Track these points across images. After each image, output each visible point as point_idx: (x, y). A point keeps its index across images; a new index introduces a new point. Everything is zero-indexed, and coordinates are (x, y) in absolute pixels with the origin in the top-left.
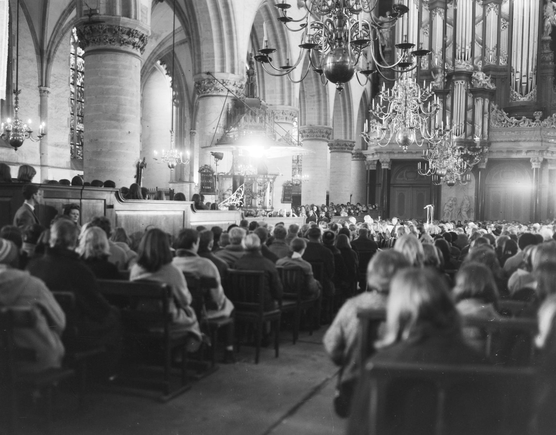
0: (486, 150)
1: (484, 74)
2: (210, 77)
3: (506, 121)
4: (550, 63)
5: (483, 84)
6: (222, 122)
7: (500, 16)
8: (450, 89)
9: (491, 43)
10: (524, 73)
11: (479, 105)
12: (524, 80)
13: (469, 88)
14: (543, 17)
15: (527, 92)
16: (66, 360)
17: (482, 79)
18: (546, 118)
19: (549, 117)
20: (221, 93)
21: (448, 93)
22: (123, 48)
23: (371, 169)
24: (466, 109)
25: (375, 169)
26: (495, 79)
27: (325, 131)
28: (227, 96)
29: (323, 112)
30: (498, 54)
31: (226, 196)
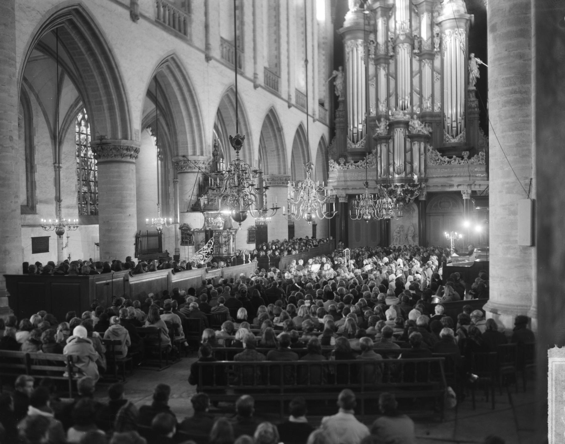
0: (423, 185)
1: (419, 122)
2: (185, 159)
4: (476, 109)
6: (195, 192)
7: (433, 69)
9: (427, 93)
10: (454, 119)
11: (416, 147)
12: (454, 124)
13: (407, 134)
14: (468, 71)
15: (457, 135)
16: (128, 356)
17: (417, 126)
19: (476, 156)
20: (194, 170)
21: (390, 138)
22: (123, 159)
24: (405, 152)
26: (431, 123)
27: (284, 179)
28: (198, 172)
29: (282, 163)
30: (433, 102)
31: (200, 246)
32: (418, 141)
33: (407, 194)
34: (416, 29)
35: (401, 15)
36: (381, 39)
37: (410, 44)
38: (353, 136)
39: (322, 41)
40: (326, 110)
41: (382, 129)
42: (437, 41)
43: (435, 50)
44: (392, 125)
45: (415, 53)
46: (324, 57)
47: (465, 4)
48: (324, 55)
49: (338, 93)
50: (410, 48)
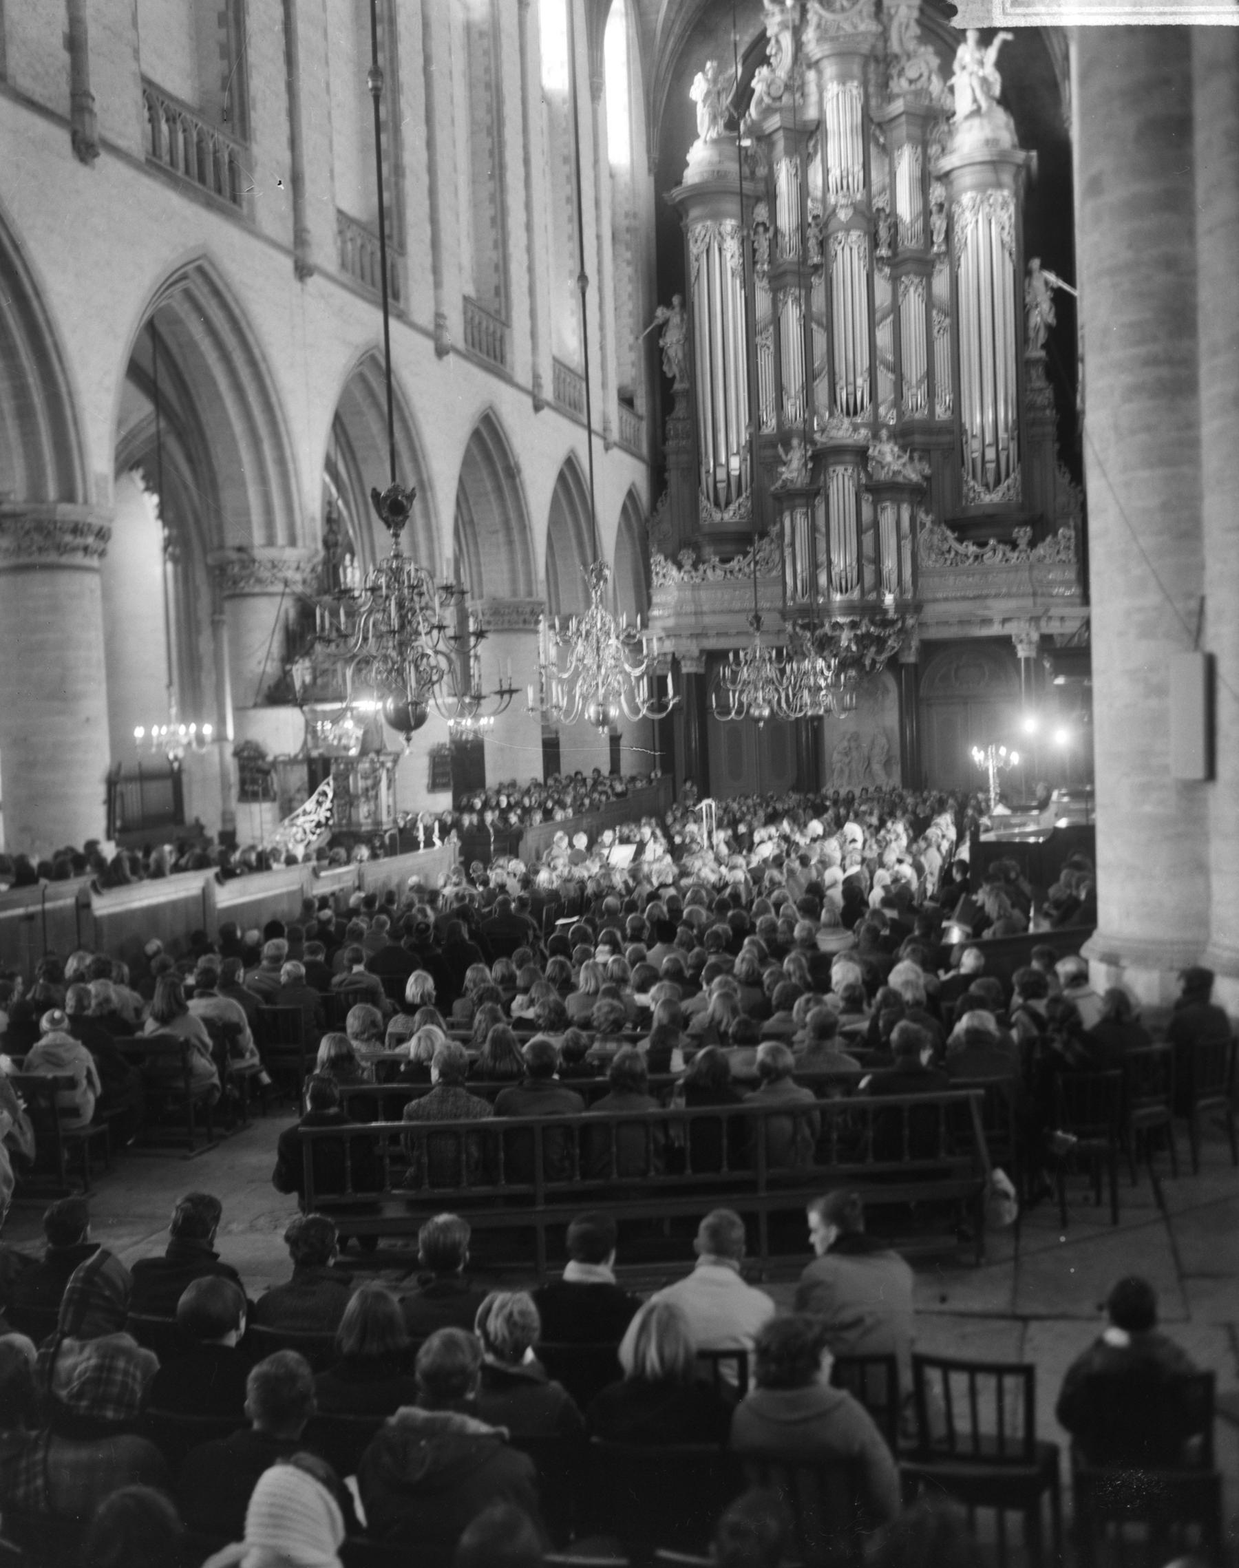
0: (910, 622)
1: (896, 449)
2: (244, 556)
3: (953, 553)
4: (1048, 412)
5: (894, 473)
7: (930, 303)
8: (821, 484)
9: (914, 367)
10: (989, 438)
11: (887, 519)
12: (990, 454)
13: (864, 481)
14: (1025, 306)
15: (998, 482)
18: (1043, 539)
19: (1049, 539)
20: (271, 589)
21: (817, 494)
22: (65, 560)
26: (929, 451)
27: (528, 609)
28: (283, 594)
29: (520, 568)
30: (931, 394)
31: (295, 804)
32: (893, 500)
33: (865, 647)
34: (883, 190)
35: (840, 152)
36: (786, 220)
39: (624, 223)
40: (640, 418)
41: (793, 469)
42: (939, 223)
43: (935, 249)
44: (822, 458)
45: (882, 258)
46: (629, 270)
47: (1012, 123)
48: (629, 263)
49: (672, 370)
50: (865, 244)
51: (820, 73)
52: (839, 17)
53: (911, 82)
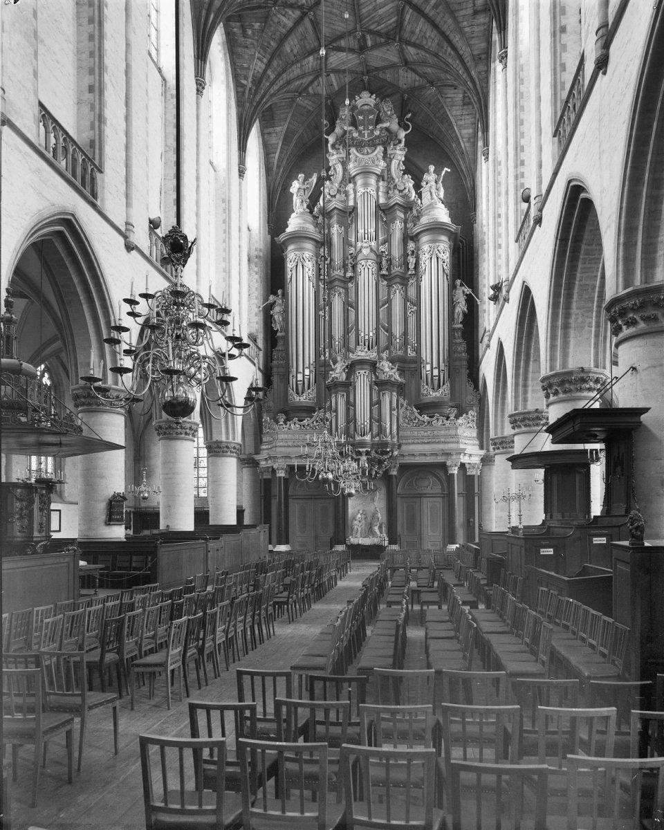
7: (406, 299)
9: (397, 330)
10: (435, 365)
11: (386, 399)
12: (436, 372)
15: (439, 386)
17: (388, 370)
19: (464, 415)
23: (265, 477)
25: (269, 477)
34: (384, 242)
37: (377, 263)
38: (297, 384)
39: (254, 253)
42: (412, 260)
43: (410, 272)
45: (383, 276)
46: (257, 277)
49: (277, 327)
51: (355, 184)
52: (366, 157)
53: (400, 191)
